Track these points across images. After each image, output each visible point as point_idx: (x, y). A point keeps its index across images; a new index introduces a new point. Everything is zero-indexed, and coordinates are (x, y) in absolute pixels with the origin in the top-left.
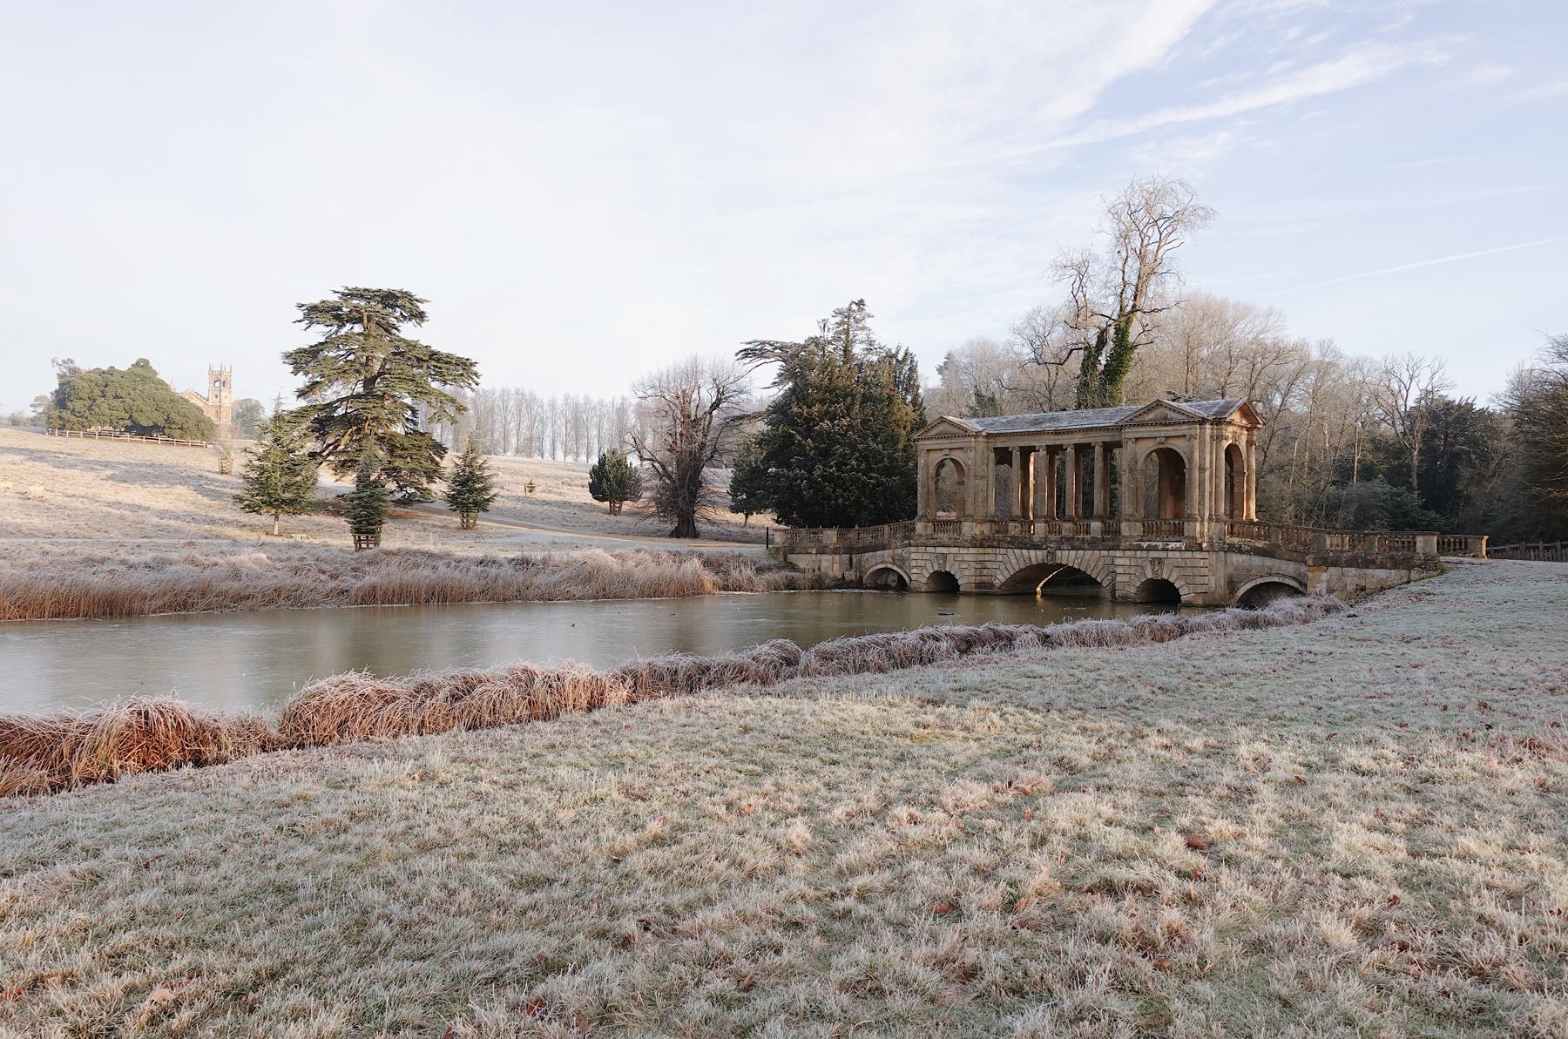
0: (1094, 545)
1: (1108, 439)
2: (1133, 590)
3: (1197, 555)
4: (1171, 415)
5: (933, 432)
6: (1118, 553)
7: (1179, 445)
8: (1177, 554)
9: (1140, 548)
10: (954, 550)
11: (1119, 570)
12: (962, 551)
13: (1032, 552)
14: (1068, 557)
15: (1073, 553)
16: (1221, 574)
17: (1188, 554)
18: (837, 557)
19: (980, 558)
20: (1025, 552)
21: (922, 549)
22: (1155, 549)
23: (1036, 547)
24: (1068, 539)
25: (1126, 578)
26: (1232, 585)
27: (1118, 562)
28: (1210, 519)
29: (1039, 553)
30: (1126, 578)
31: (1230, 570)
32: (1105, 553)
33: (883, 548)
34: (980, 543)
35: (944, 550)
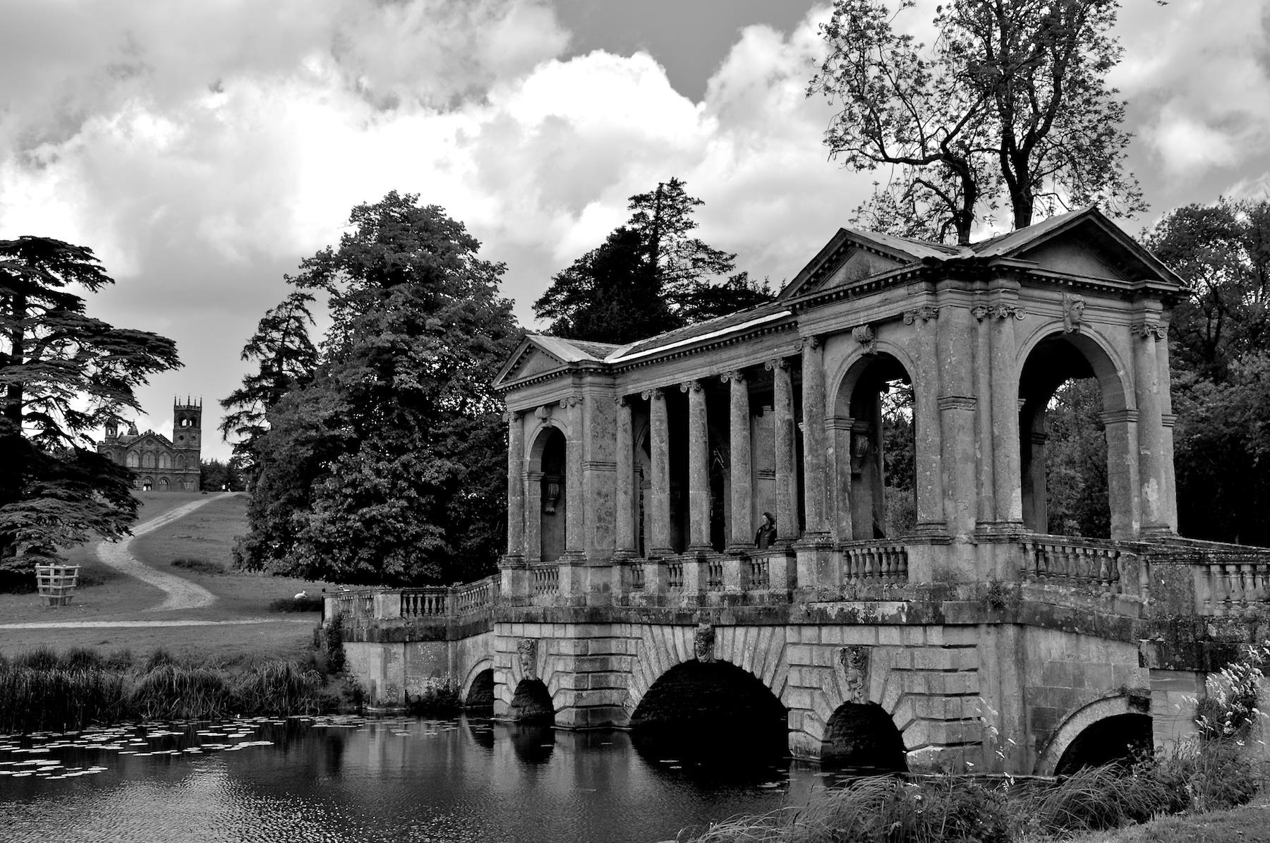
3: (936, 636)
5: (525, 373)
6: (791, 634)
7: (894, 342)
8: (890, 636)
9: (822, 621)
10: (547, 630)
12: (559, 632)
13: (678, 630)
14: (736, 647)
15: (740, 631)
16: (1012, 689)
17: (916, 635)
18: (398, 649)
19: (593, 647)
20: (667, 630)
22: (849, 620)
23: (683, 620)
24: (733, 599)
26: (1042, 725)
28: (978, 538)
29: (690, 634)
31: (1035, 680)
34: (594, 617)
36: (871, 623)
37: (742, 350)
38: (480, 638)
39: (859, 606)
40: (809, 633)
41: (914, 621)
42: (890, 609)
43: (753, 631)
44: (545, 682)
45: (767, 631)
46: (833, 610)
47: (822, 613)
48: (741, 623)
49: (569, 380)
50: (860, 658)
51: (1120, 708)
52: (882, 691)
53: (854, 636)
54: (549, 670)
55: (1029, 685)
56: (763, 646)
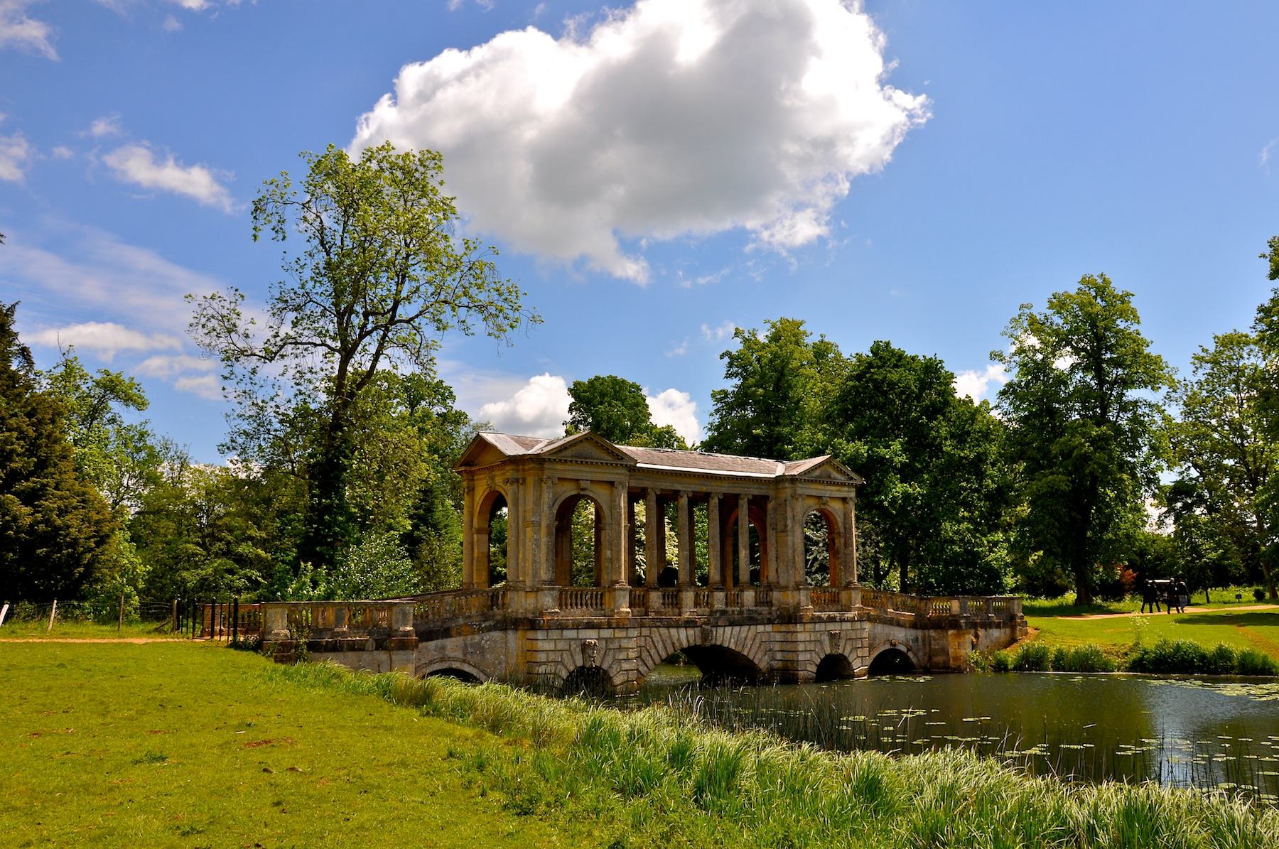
0: (751, 620)
1: (756, 492)
2: (814, 669)
4: (835, 474)
9: (820, 620)
10: (606, 633)
11: (801, 647)
13: (682, 631)
14: (727, 637)
15: (728, 629)
17: (858, 625)
20: (673, 631)
21: (555, 634)
22: (832, 620)
23: (689, 624)
24: (723, 612)
25: (808, 656)
27: (801, 637)
29: (691, 632)
30: (808, 656)
32: (761, 628)
33: (446, 633)
35: (591, 636)
36: (842, 621)
37: (726, 484)
38: (432, 644)
39: (837, 614)
40: (809, 627)
41: (860, 620)
42: (850, 615)
43: (737, 628)
44: (605, 666)
45: (746, 628)
46: (824, 615)
47: (820, 617)
48: (732, 624)
49: (624, 471)
50: (833, 637)
51: (888, 647)
52: (844, 649)
53: (832, 627)
54: (609, 660)
55: (1008, 631)
56: (743, 635)
